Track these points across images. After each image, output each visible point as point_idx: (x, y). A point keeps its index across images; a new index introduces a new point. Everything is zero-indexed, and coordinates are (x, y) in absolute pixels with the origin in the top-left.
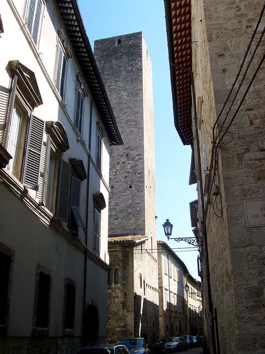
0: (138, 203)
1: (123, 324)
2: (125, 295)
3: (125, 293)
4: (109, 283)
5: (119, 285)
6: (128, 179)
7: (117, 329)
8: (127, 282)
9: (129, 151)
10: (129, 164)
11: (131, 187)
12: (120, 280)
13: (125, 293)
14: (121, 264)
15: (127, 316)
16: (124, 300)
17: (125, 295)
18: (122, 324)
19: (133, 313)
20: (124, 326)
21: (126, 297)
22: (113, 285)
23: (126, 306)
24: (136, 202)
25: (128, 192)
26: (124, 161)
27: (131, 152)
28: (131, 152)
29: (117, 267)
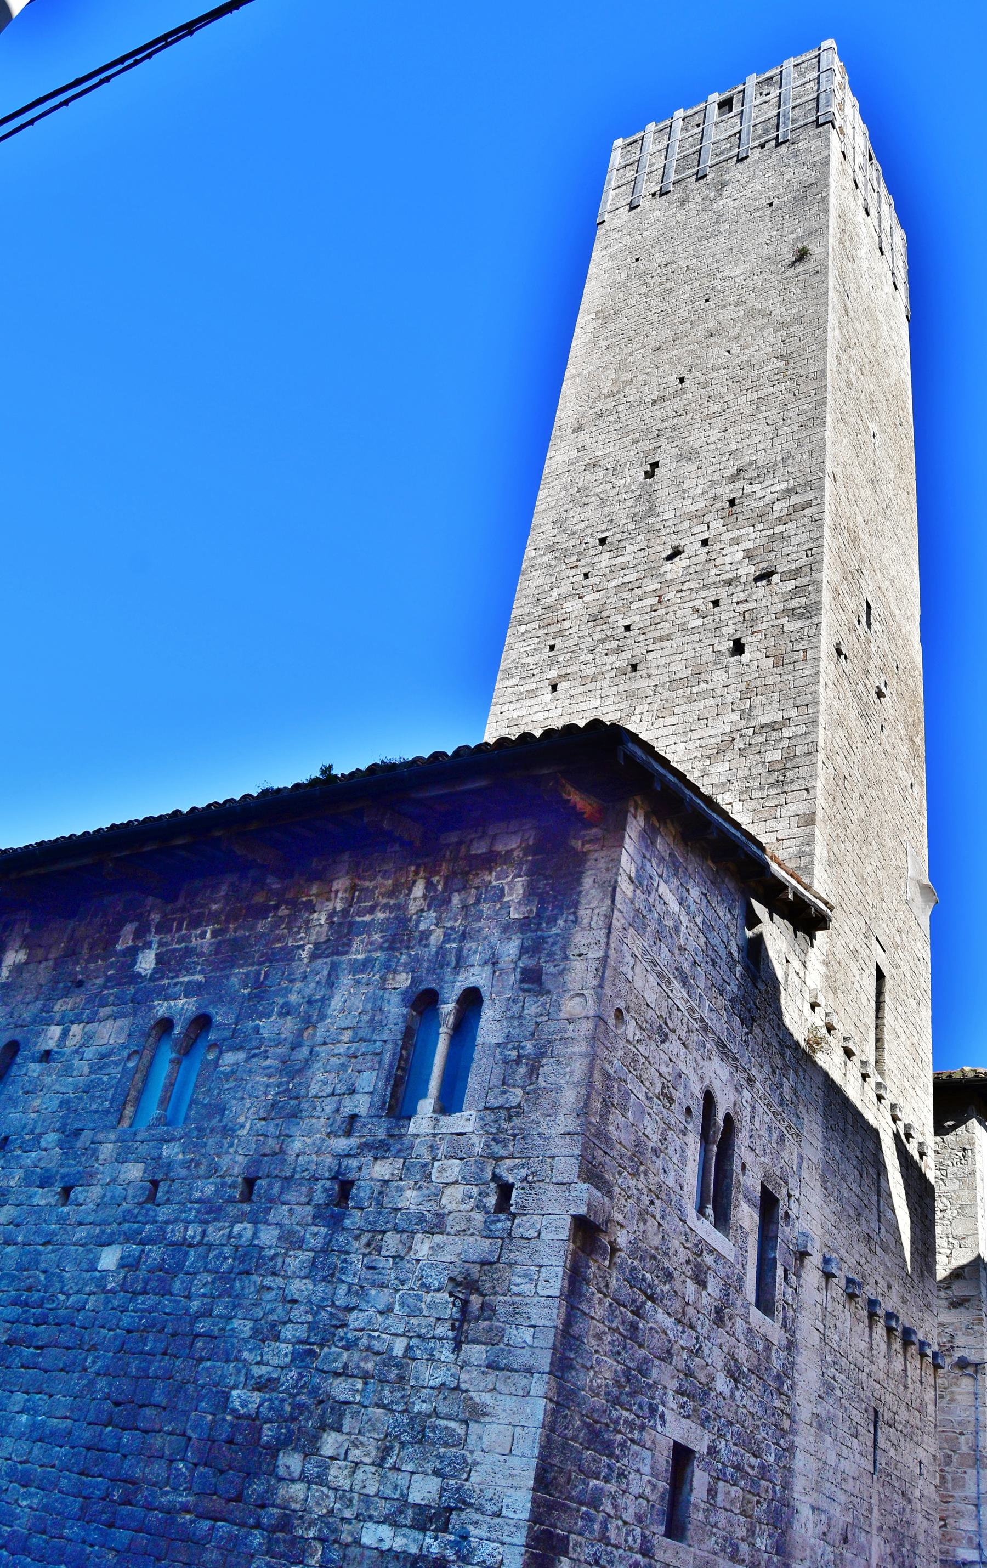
0: (772, 726)
1: (434, 1484)
2: (503, 1204)
3: (505, 1190)
4: (398, 1105)
5: (465, 1121)
6: (725, 613)
7: (375, 1535)
8: (533, 1094)
9: (739, 485)
10: (736, 541)
11: (738, 648)
12: (480, 1076)
13: (505, 1190)
14: (510, 949)
15: (476, 1413)
16: (480, 1247)
17: (503, 1204)
18: (424, 1490)
19: (539, 1385)
20: (431, 1518)
21: (502, 1224)
22: (423, 1121)
23: (488, 1310)
24: (765, 720)
25: (719, 676)
26: (706, 535)
27: (748, 490)
28: (748, 490)
29: (477, 976)
